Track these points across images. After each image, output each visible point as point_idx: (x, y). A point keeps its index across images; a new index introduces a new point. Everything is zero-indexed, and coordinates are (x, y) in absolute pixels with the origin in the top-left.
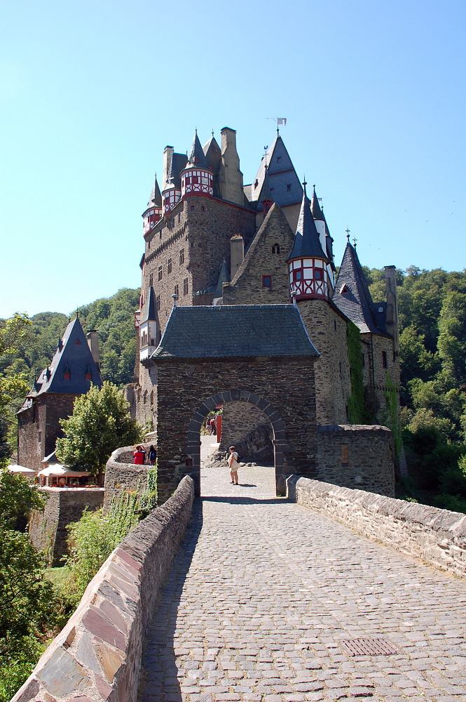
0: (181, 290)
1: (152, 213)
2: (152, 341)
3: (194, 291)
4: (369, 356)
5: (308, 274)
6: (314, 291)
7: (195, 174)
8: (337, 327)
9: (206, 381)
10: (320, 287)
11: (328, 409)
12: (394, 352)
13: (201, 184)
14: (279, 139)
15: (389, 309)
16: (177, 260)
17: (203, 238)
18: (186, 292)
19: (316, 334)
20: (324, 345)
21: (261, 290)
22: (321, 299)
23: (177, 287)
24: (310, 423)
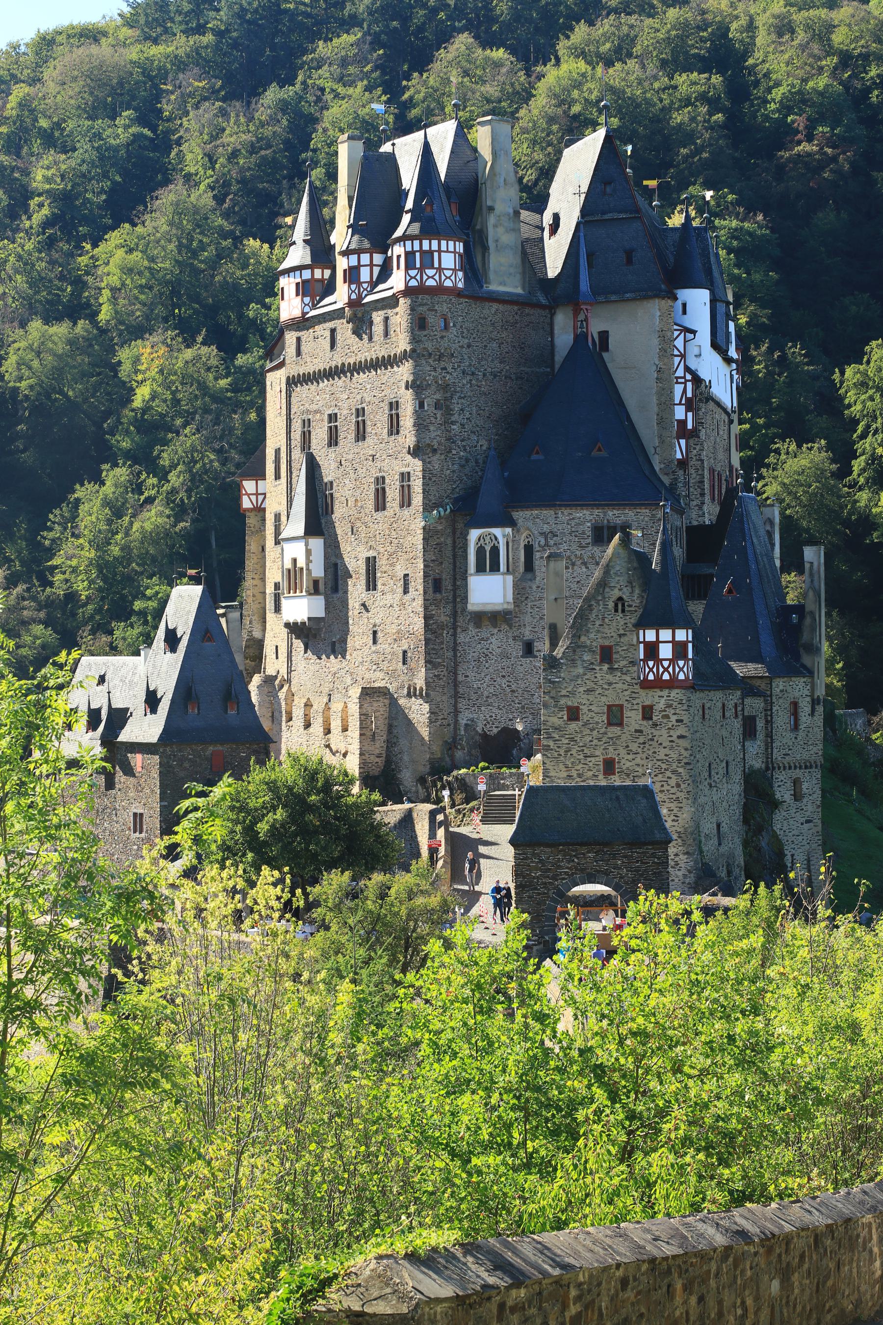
0: (393, 494)
1: (307, 274)
2: (316, 583)
3: (428, 507)
4: (766, 715)
5: (666, 651)
7: (426, 245)
8: (707, 712)
10: (681, 669)
12: (813, 700)
13: (440, 269)
15: (808, 621)
16: (378, 423)
17: (445, 387)
18: (406, 501)
19: (674, 738)
20: (686, 754)
23: (380, 480)
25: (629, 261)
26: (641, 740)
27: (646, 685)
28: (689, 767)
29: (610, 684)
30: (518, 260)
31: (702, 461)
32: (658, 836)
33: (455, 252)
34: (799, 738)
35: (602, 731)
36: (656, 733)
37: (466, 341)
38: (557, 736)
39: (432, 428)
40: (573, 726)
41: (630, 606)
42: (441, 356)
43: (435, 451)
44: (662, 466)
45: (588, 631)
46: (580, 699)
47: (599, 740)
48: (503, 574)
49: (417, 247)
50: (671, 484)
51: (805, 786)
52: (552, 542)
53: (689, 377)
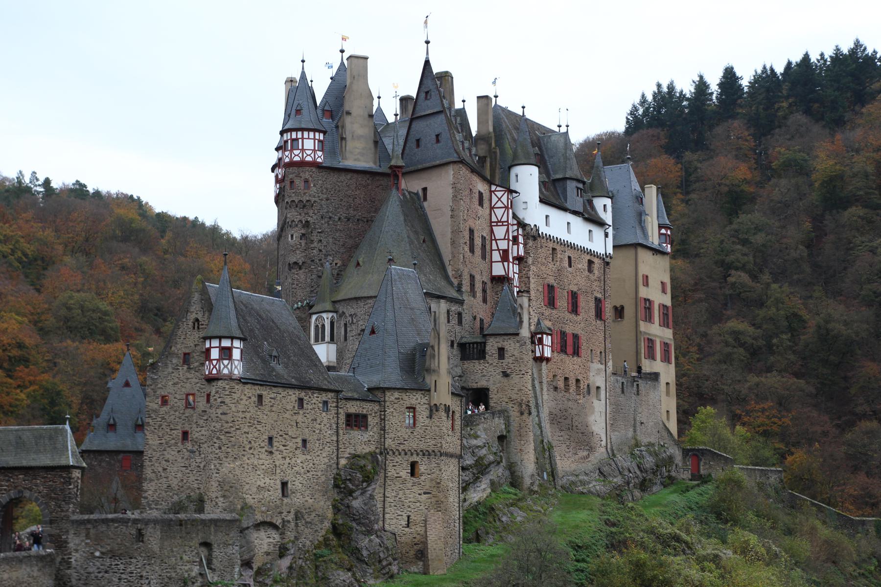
4: (381, 415)
5: (215, 354)
6: (219, 371)
7: (294, 136)
8: (266, 400)
9: (3, 483)
10: (226, 367)
11: (225, 489)
12: (430, 407)
13: (303, 150)
14: (427, 63)
15: (430, 351)
20: (226, 425)
21: (181, 368)
22: (225, 379)
24: (65, 514)
25: (438, 141)
26: (205, 418)
27: (211, 380)
28: (228, 435)
29: (188, 379)
30: (371, 145)
31: (529, 278)
32: (63, 462)
33: (314, 139)
34: (415, 434)
35: (181, 412)
36: (211, 411)
37: (325, 196)
38: (152, 415)
39: (298, 252)
40: (165, 408)
41: (202, 325)
42: (304, 206)
43: (300, 268)
44: (454, 272)
45: (176, 343)
46: (168, 389)
47: (180, 418)
48: (329, 343)
49: (289, 138)
50: (459, 284)
51: (422, 468)
52: (355, 321)
53: (515, 222)
